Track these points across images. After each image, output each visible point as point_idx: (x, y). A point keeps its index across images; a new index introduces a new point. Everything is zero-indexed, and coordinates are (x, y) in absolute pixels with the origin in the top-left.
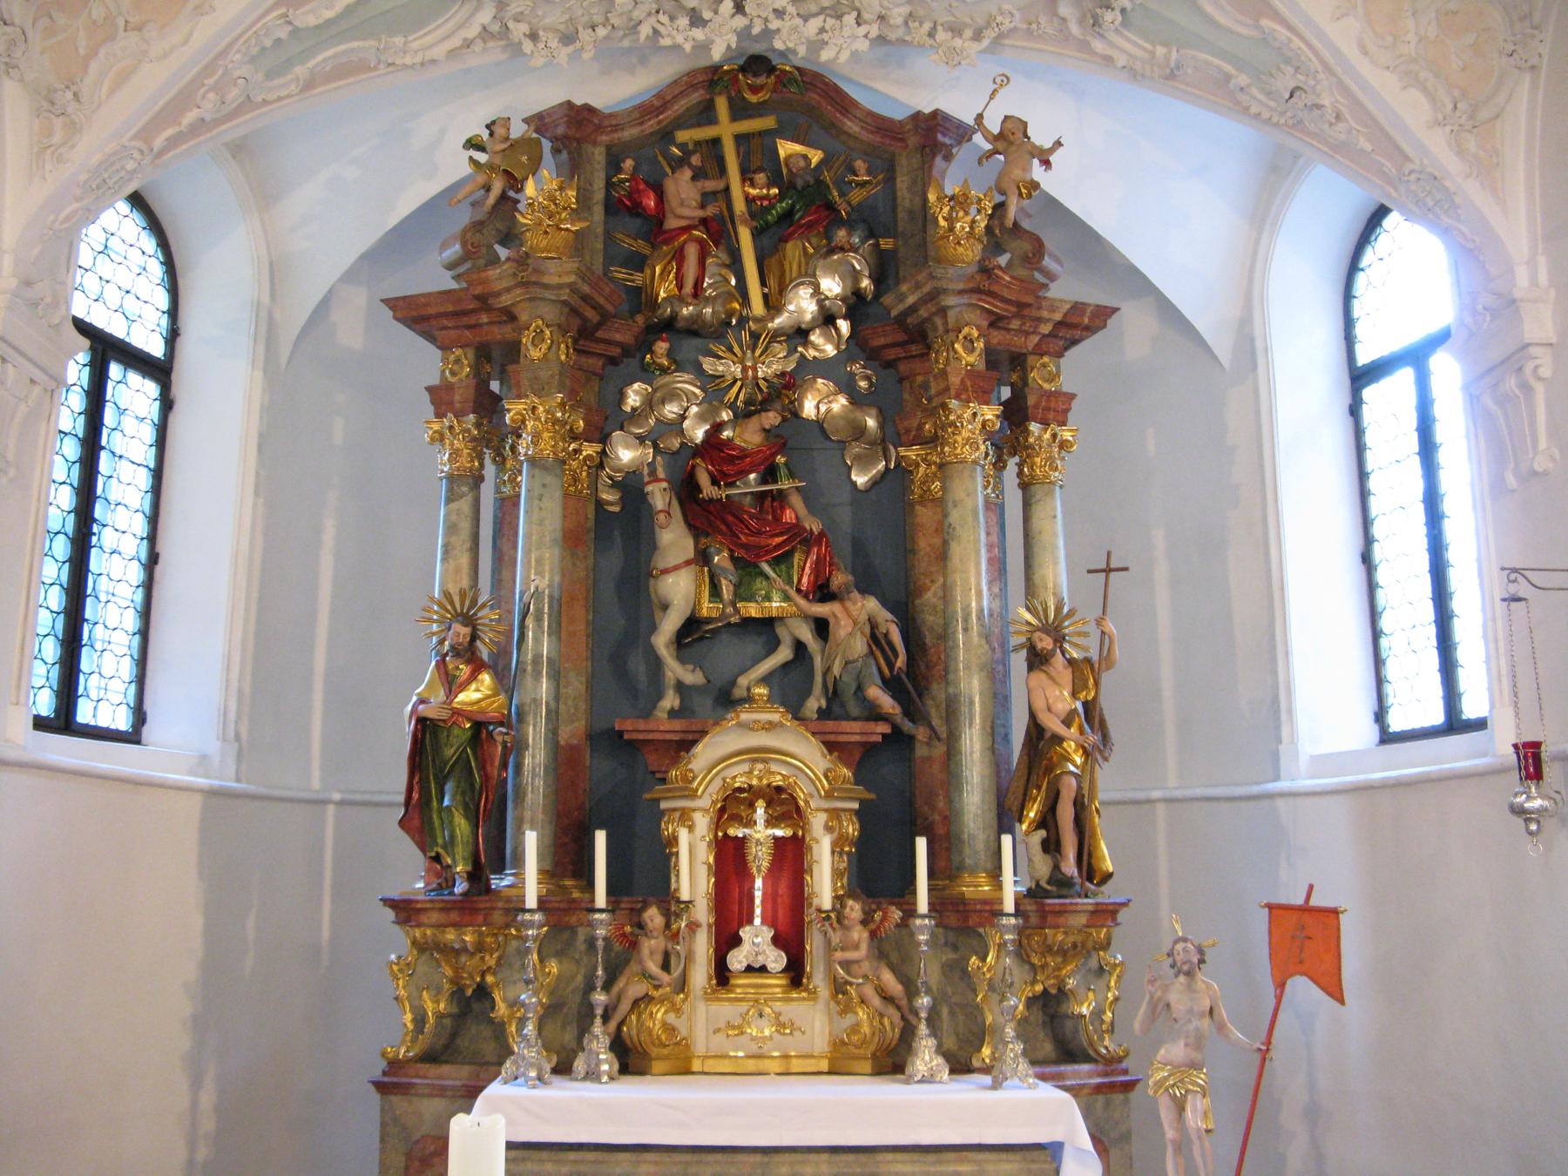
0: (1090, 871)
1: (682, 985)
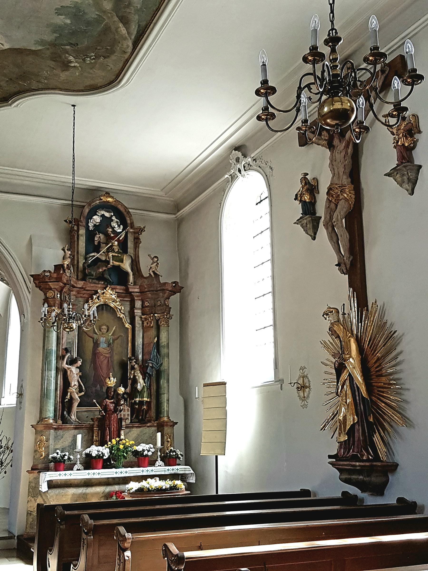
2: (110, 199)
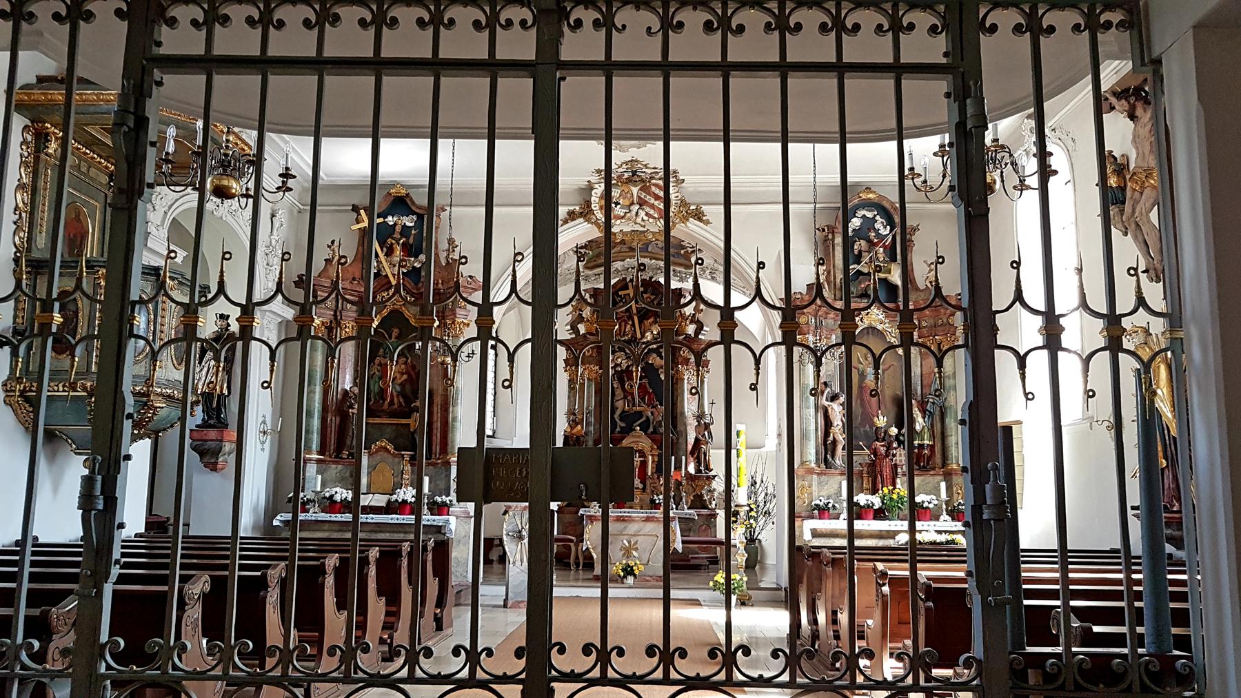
0: (708, 468)
2: (871, 196)
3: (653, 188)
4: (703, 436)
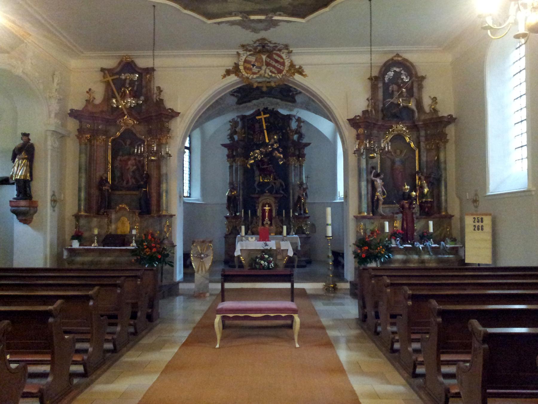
1: (258, 226)
2: (400, 59)
3: (275, 56)
4: (303, 195)
